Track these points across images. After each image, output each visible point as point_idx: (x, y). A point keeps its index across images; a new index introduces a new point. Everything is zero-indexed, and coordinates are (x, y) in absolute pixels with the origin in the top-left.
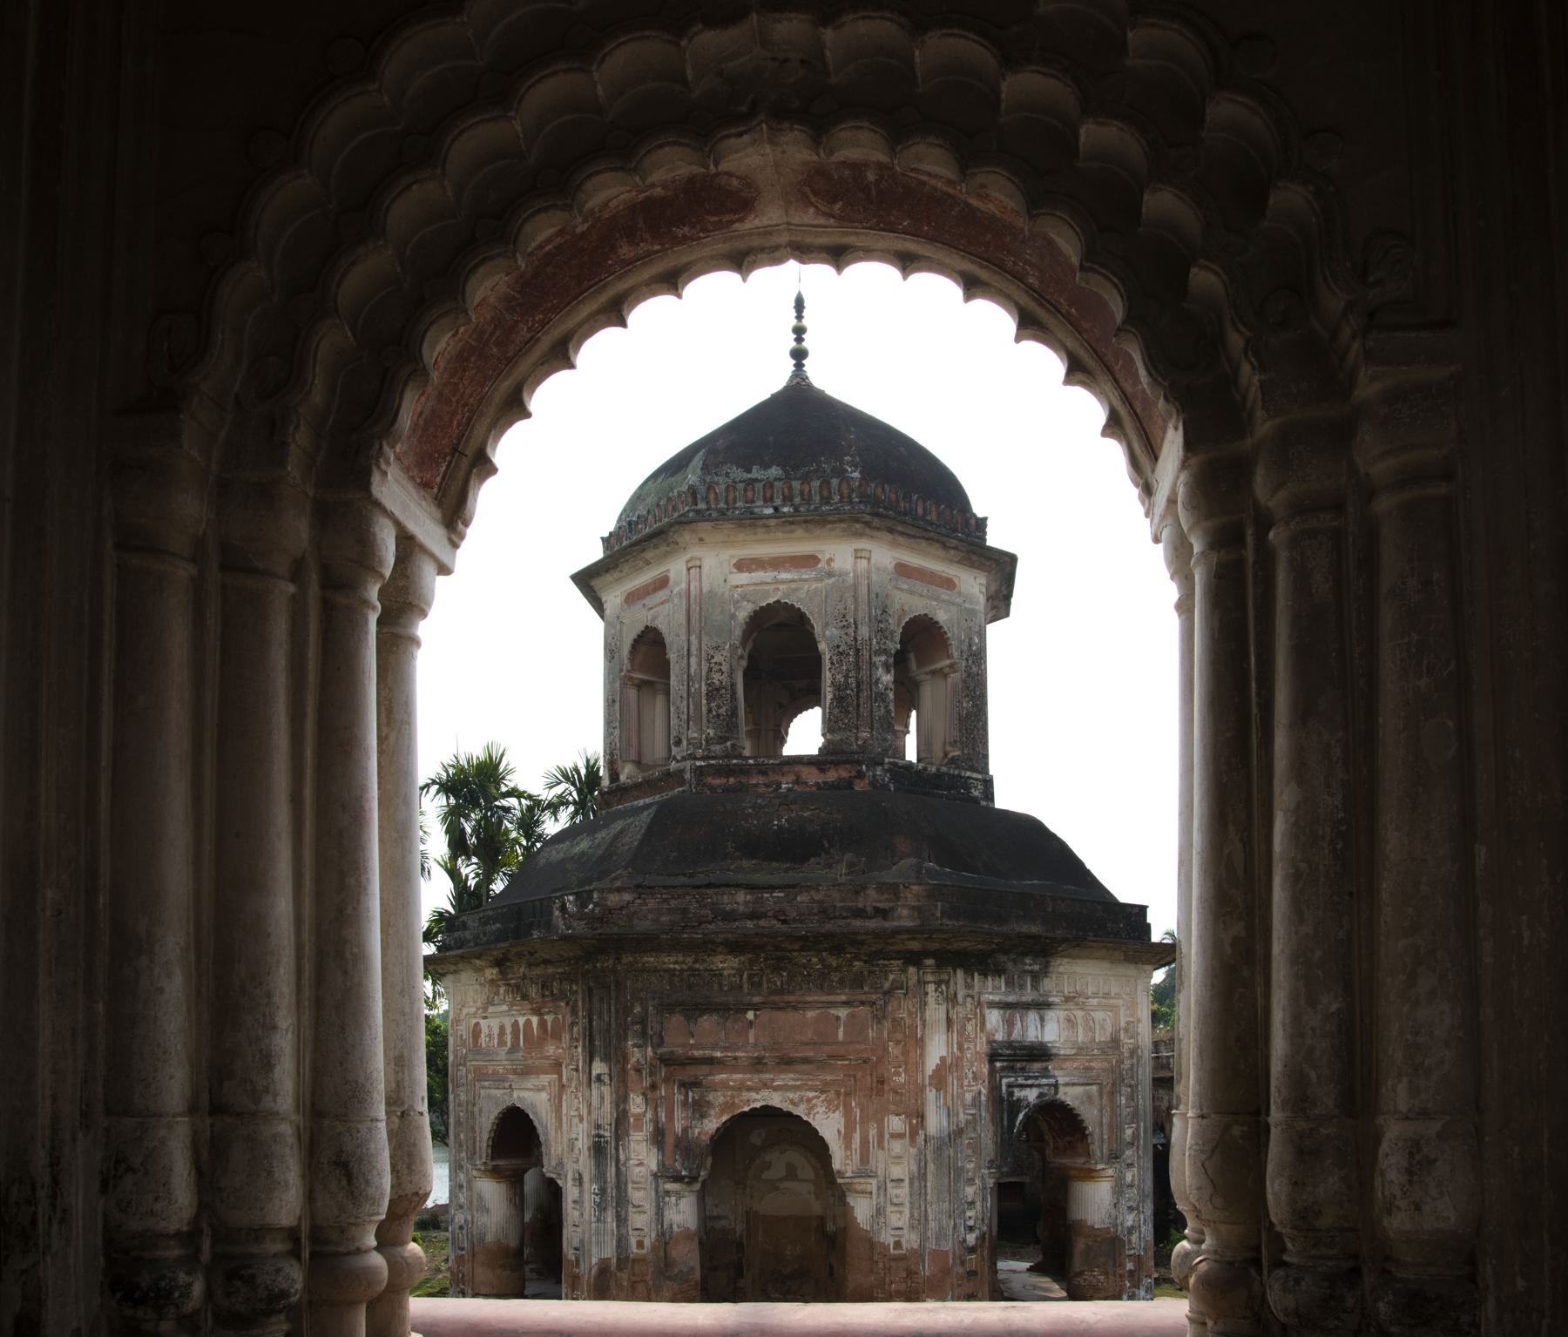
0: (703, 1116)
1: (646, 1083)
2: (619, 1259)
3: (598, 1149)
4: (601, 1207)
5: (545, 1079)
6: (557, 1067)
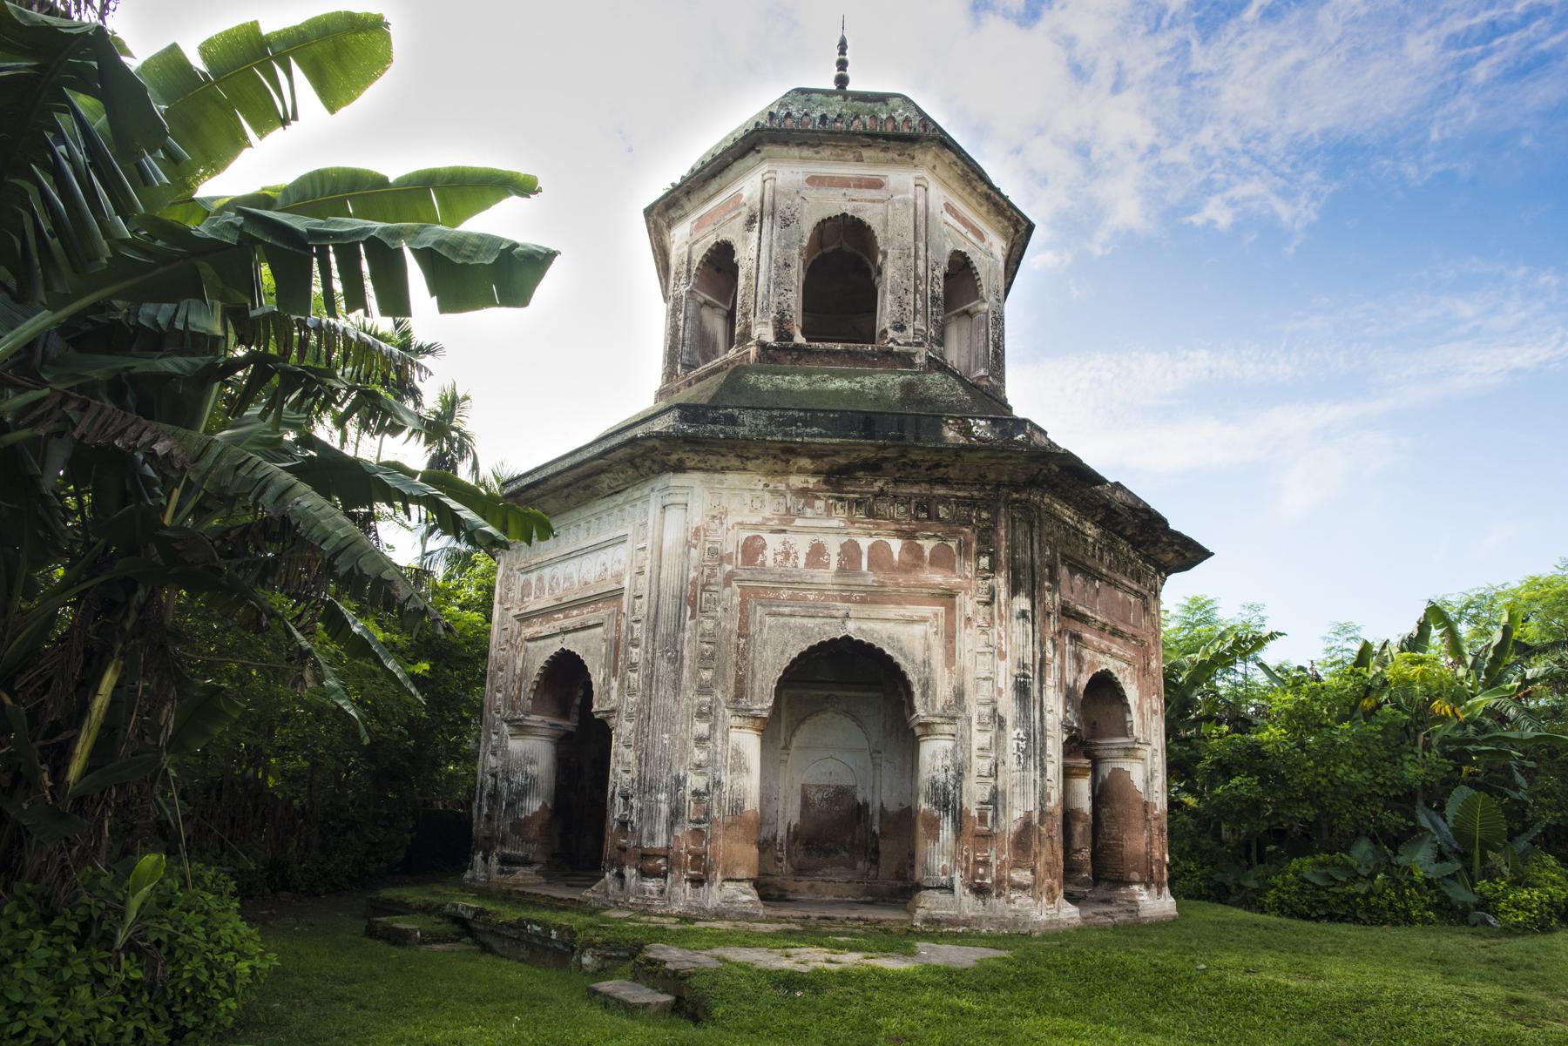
0: (1080, 671)
1: (1053, 627)
2: (1042, 812)
3: (1022, 690)
4: (1025, 754)
5: (927, 610)
6: (948, 597)
